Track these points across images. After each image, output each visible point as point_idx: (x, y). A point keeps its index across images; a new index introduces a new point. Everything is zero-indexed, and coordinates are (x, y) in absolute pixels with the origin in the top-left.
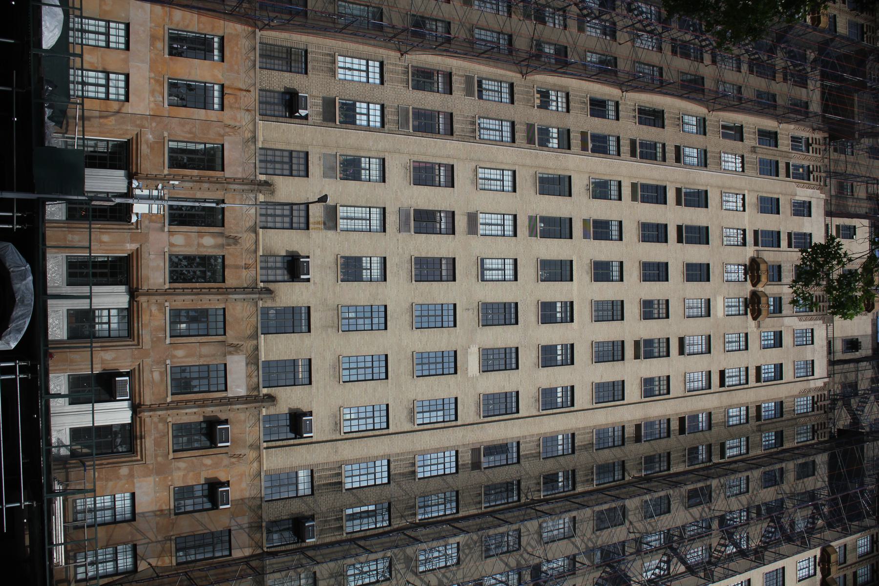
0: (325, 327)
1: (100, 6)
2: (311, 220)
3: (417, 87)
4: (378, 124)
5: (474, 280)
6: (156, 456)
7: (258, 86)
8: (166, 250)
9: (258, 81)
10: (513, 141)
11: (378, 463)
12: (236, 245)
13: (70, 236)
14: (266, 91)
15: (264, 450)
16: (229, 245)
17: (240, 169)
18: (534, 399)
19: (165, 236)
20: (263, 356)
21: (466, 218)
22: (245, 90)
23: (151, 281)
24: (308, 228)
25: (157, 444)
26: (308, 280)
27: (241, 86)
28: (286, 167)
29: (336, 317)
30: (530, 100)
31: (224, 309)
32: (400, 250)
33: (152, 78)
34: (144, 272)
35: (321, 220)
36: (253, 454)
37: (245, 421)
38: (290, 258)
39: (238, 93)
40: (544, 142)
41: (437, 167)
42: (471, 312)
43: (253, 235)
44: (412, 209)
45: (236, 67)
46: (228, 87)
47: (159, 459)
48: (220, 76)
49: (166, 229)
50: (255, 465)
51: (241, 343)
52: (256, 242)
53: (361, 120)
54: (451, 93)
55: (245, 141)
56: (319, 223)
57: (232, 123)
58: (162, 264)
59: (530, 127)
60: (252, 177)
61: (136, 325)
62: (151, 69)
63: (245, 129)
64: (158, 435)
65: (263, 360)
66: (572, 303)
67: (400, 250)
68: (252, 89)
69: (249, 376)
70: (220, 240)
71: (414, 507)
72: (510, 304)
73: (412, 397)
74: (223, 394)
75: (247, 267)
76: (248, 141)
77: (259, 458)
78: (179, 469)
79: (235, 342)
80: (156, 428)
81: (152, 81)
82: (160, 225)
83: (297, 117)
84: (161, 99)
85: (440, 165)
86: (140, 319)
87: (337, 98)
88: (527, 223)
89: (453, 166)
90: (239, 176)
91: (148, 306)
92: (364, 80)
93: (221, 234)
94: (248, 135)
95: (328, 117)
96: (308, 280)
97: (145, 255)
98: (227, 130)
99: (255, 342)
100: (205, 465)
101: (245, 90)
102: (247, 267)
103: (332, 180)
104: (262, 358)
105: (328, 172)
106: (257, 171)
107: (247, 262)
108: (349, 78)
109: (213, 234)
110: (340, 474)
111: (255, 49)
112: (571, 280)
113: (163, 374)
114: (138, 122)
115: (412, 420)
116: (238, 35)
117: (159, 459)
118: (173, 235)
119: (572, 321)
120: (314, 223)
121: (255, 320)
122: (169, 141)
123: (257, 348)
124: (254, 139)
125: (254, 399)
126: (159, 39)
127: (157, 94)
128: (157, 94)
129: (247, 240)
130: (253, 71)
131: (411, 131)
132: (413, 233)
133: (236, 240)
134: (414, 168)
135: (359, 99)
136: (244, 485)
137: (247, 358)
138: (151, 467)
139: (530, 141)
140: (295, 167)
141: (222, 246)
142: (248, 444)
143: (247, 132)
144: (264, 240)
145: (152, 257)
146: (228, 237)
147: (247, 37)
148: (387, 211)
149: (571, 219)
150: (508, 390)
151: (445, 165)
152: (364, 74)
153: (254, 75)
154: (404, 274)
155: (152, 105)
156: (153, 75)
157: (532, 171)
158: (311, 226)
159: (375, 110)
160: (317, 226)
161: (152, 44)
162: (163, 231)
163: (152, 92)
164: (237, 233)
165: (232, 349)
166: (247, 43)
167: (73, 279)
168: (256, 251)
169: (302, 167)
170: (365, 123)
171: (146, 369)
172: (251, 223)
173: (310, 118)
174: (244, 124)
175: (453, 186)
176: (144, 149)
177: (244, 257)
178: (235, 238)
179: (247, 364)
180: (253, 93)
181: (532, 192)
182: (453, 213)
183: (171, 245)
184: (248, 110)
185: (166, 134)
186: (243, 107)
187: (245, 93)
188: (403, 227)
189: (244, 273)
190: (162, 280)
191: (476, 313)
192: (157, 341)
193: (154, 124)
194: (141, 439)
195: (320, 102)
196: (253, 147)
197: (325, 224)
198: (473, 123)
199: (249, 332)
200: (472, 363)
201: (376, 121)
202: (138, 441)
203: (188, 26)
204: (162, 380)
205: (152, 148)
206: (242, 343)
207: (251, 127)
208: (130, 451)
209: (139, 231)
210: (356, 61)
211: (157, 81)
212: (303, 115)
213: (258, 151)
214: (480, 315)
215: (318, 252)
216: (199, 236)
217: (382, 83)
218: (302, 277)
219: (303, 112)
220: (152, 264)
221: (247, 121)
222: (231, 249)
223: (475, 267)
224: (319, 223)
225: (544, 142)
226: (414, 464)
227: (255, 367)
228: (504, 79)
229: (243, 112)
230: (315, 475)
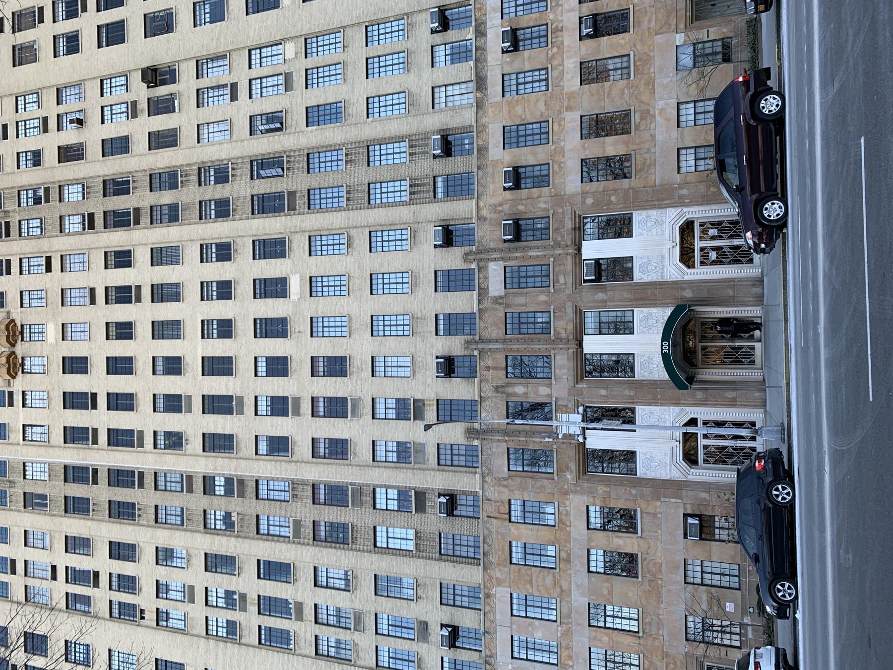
0: (423, 318)
1: (612, 586)
2: (435, 407)
3: (344, 527)
4: (378, 490)
5: (294, 357)
6: (563, 213)
7: (481, 521)
9: (481, 526)
10: (257, 481)
11: (378, 201)
14: (474, 517)
16: (503, 387)
17: (494, 450)
18: (239, 251)
19: (555, 394)
21: (301, 412)
22: (491, 517)
23: (566, 357)
24: (438, 400)
25: (562, 222)
26: (437, 357)
27: (495, 521)
28: (455, 452)
29: (414, 327)
30: (241, 519)
31: (506, 334)
32: (359, 383)
34: (571, 364)
35: (427, 408)
36: (484, 213)
37: (490, 241)
38: (452, 375)
39: (497, 515)
40: (229, 481)
41: (327, 455)
42: (297, 330)
43: (483, 395)
44: (349, 418)
45: (499, 537)
46: (505, 519)
47: (561, 211)
48: (512, 529)
49: (554, 399)
50: (482, 204)
52: (480, 390)
53: (393, 494)
54: (314, 522)
56: (429, 405)
57: (502, 489)
58: (557, 371)
59: (241, 495)
60: (484, 442)
62: (569, 533)
64: (561, 230)
66: (203, 337)
67: (359, 383)
68: (486, 519)
69: (486, 278)
70: (510, 390)
71: (347, 162)
72: (261, 337)
73: (350, 259)
74: (507, 264)
75: (488, 368)
76: (488, 474)
77: (478, 209)
78: (545, 202)
79: (497, 306)
80: (562, 237)
81: (568, 524)
82: (559, 403)
83: (447, 495)
84: (560, 508)
85: (325, 457)
87: (414, 513)
88: (245, 408)
89: (313, 457)
90: (495, 444)
91: (568, 336)
92: (390, 530)
93: (508, 395)
95: (421, 497)
96: (437, 357)
97: (571, 378)
98: (505, 483)
99: (481, 307)
100: (523, 205)
101: (491, 517)
102: (488, 368)
103: (418, 441)
104: (475, 294)
105: (420, 448)
106: (480, 449)
107: (487, 372)
108: (403, 531)
109: (516, 395)
110: (412, 193)
111: (484, 554)
112: (203, 358)
113: (556, 281)
114: (579, 489)
115: (349, 238)
116: (498, 565)
117: (561, 211)
119: (203, 321)
120: (432, 405)
121: (480, 325)
122: (553, 473)
123: (480, 302)
124: (483, 476)
125: (482, 256)
126: (564, 560)
127: (564, 512)
128: (564, 512)
129: (488, 390)
130: (485, 534)
131: (350, 487)
132: (349, 398)
134: (348, 454)
135: (395, 513)
136: (492, 187)
137: (488, 293)
138: (568, 204)
139: (241, 482)
140: (449, 452)
141: (509, 385)
142: (487, 222)
144: (474, 391)
145: (565, 377)
146: (503, 393)
147: (491, 563)
148: (371, 416)
149: (203, 413)
150: (263, 261)
151: (319, 457)
152: (390, 535)
154: (356, 362)
155: (568, 503)
156: (568, 528)
157: (240, 455)
158: (435, 402)
159: (381, 503)
160: (430, 402)
161: (569, 555)
162: (556, 398)
163: (568, 514)
164: (496, 397)
165: (500, 301)
168: (481, 381)
169: (442, 451)
170: (390, 491)
171: (570, 285)
172: (484, 404)
173: (437, 494)
175: (313, 439)
176: (573, 466)
178: (498, 392)
179: (488, 288)
180: (485, 515)
181: (240, 436)
182: (313, 416)
183: (550, 386)
184: (489, 500)
186: (493, 503)
187: (492, 515)
188: (357, 402)
189: (490, 363)
190: (557, 357)
191: (293, 329)
192: (560, 308)
193: (566, 487)
195: (429, 510)
196: (484, 468)
197: (424, 404)
198: (294, 496)
200: (296, 286)
201: (380, 494)
203: (540, 571)
204: (557, 276)
205: (568, 468)
207: (486, 486)
210: (398, 547)
211: (564, 524)
212: (442, 497)
213: (480, 465)
214: (289, 328)
215: (429, 381)
217: (375, 528)
218: (442, 360)
219: (443, 500)
220: (565, 371)
222: (500, 383)
223: (293, 368)
224: (429, 405)
225: (229, 481)
226: (348, 199)
227: (481, 286)
228: (265, 537)
229: (492, 499)
230: (432, 193)
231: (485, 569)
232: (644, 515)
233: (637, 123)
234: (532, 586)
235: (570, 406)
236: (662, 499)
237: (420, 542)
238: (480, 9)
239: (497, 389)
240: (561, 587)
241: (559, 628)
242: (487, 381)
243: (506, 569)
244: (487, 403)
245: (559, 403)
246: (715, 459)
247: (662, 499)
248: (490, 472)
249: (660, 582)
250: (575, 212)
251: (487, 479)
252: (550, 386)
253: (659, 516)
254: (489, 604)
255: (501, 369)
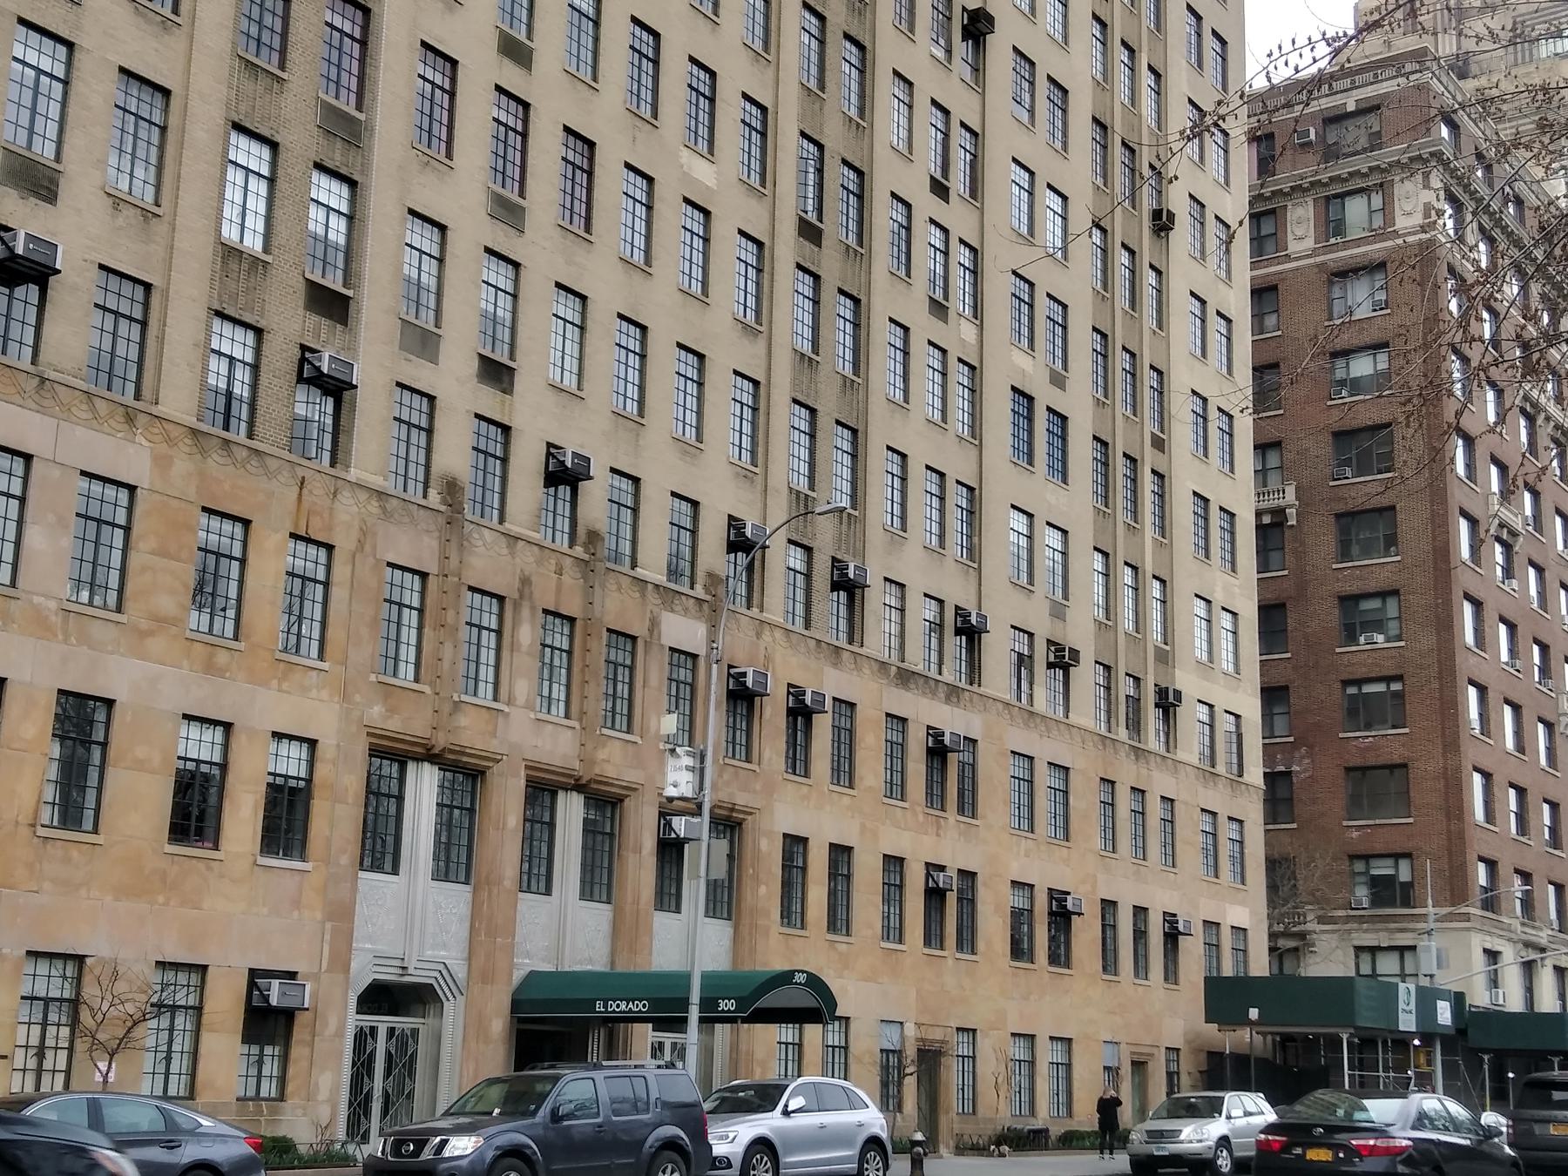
8: (532, 716)
12: (530, 584)
13: (505, 883)
15: (507, 525)
20: (188, 418)
33: (279, 685)
36: (767, 635)
39: (305, 505)
46: (296, 525)
49: (506, 709)
51: (648, 615)
55: (382, 516)
61: (613, 790)
62: (265, 684)
63: (363, 510)
65: (665, 578)
68: (300, 472)
70: (525, 612)
75: (559, 572)
76: (383, 509)
78: (770, 759)
81: (285, 686)
82: (501, 719)
84: (314, 673)
86: (611, 781)
87: (308, 276)
94: (374, 506)
98: (368, 548)
99: (650, 587)
117: (758, 787)
118: (515, 699)
124: (381, 495)
133: (525, 581)
141: (533, 608)
143: (369, 507)
145: (539, 745)
146: (521, 597)
147: (204, 453)
153: (275, 460)
155: (325, 694)
156: (275, 682)
163: (304, 690)
166: (215, 456)
167: (209, 832)
174: (355, 509)
176: (394, 725)
177: (546, 572)
179: (672, 611)
180: (308, 474)
185: (373, 678)
190: (569, 733)
194: (732, 810)
196: (395, 502)
199: (637, 595)
202: (734, 815)
205: (392, 711)
206: (648, 611)
208: (474, 778)
209: (504, 757)
216: (519, 651)
221: (352, 501)
229: (337, 504)
231: (194, 432)
232: (297, 877)
233: (837, 945)
234: (153, 553)
235: (495, 742)
236: (328, 925)
237: (245, 266)
238: (971, 701)
239: (525, 581)
240: (150, 633)
241: (53, 605)
242: (539, 563)
243: (192, 493)
244: (505, 551)
245: (501, 719)
246: (393, 1052)
247: (328, 925)
248: (386, 514)
249: (161, 899)
250: (751, 814)
251: (376, 504)
252: (529, 706)
253: (296, 914)
254: (111, 415)
255: (557, 603)
